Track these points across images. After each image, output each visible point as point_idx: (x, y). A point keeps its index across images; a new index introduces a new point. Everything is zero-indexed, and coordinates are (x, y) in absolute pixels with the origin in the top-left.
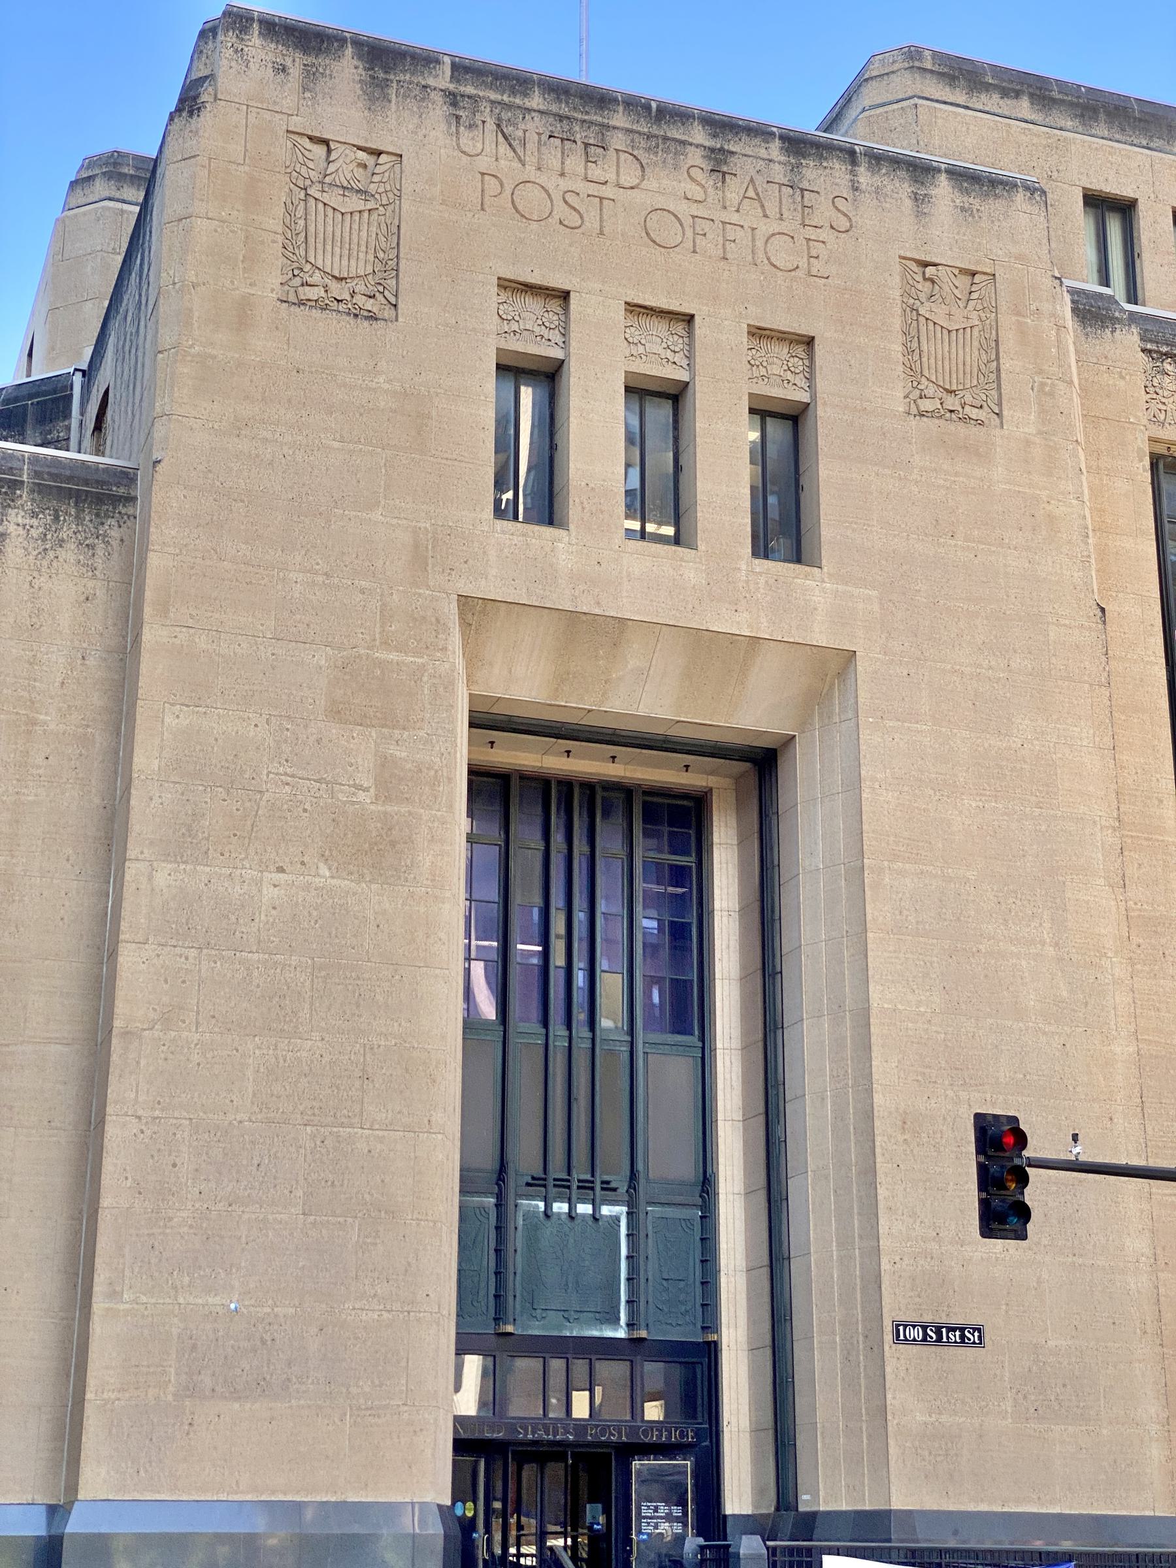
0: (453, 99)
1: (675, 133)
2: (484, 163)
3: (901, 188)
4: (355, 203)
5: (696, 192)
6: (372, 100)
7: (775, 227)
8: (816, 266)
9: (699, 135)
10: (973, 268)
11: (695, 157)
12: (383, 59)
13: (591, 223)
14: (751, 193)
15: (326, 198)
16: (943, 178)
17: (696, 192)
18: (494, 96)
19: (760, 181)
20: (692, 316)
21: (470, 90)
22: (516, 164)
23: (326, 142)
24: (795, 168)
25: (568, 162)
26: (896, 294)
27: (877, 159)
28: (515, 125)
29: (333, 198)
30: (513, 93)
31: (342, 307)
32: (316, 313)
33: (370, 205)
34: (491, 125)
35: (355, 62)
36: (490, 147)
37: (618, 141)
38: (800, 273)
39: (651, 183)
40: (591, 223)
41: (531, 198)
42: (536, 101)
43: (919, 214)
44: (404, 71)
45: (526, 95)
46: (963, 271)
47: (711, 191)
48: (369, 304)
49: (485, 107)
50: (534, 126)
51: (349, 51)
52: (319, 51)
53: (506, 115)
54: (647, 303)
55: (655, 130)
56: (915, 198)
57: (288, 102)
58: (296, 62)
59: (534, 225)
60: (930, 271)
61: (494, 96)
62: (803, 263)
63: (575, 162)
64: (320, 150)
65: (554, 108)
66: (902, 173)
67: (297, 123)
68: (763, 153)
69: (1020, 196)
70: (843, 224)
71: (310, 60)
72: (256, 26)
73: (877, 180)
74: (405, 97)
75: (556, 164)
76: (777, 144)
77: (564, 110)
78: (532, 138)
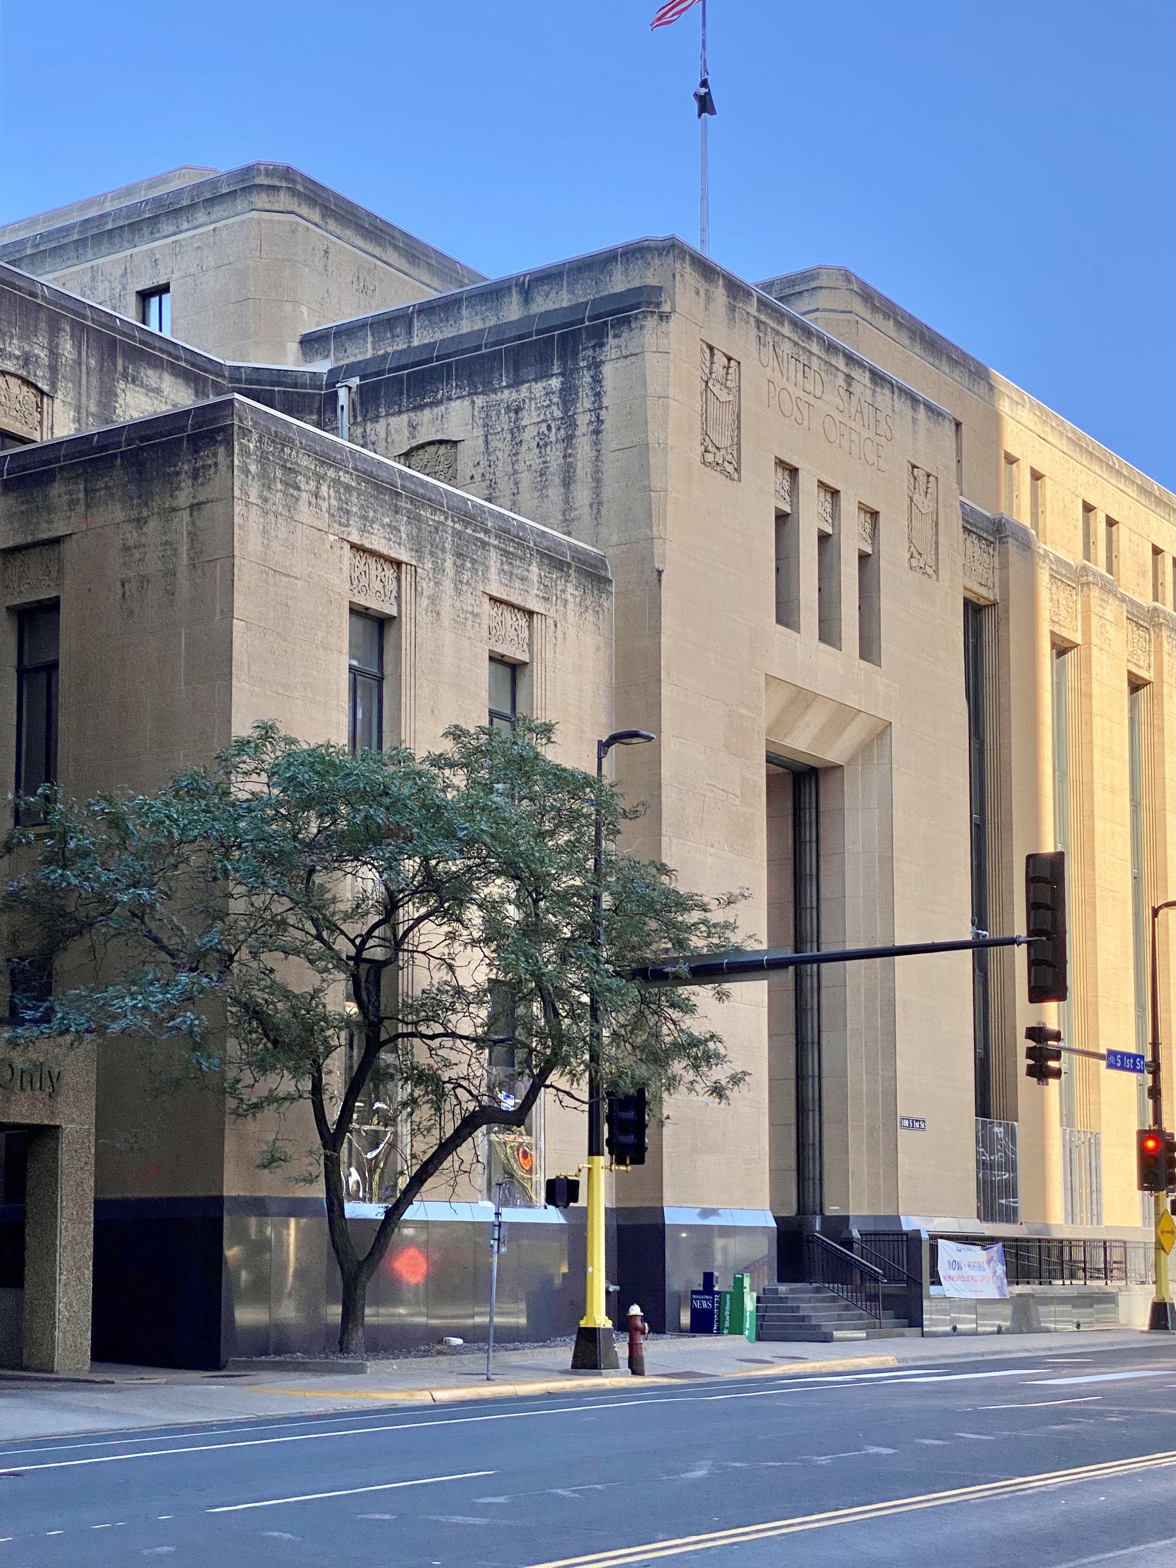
20: (838, 491)
21: (763, 318)
23: (711, 348)
31: (719, 469)
38: (875, 467)
40: (806, 423)
45: (782, 324)
50: (786, 348)
53: (777, 339)
66: (909, 402)
76: (867, 374)
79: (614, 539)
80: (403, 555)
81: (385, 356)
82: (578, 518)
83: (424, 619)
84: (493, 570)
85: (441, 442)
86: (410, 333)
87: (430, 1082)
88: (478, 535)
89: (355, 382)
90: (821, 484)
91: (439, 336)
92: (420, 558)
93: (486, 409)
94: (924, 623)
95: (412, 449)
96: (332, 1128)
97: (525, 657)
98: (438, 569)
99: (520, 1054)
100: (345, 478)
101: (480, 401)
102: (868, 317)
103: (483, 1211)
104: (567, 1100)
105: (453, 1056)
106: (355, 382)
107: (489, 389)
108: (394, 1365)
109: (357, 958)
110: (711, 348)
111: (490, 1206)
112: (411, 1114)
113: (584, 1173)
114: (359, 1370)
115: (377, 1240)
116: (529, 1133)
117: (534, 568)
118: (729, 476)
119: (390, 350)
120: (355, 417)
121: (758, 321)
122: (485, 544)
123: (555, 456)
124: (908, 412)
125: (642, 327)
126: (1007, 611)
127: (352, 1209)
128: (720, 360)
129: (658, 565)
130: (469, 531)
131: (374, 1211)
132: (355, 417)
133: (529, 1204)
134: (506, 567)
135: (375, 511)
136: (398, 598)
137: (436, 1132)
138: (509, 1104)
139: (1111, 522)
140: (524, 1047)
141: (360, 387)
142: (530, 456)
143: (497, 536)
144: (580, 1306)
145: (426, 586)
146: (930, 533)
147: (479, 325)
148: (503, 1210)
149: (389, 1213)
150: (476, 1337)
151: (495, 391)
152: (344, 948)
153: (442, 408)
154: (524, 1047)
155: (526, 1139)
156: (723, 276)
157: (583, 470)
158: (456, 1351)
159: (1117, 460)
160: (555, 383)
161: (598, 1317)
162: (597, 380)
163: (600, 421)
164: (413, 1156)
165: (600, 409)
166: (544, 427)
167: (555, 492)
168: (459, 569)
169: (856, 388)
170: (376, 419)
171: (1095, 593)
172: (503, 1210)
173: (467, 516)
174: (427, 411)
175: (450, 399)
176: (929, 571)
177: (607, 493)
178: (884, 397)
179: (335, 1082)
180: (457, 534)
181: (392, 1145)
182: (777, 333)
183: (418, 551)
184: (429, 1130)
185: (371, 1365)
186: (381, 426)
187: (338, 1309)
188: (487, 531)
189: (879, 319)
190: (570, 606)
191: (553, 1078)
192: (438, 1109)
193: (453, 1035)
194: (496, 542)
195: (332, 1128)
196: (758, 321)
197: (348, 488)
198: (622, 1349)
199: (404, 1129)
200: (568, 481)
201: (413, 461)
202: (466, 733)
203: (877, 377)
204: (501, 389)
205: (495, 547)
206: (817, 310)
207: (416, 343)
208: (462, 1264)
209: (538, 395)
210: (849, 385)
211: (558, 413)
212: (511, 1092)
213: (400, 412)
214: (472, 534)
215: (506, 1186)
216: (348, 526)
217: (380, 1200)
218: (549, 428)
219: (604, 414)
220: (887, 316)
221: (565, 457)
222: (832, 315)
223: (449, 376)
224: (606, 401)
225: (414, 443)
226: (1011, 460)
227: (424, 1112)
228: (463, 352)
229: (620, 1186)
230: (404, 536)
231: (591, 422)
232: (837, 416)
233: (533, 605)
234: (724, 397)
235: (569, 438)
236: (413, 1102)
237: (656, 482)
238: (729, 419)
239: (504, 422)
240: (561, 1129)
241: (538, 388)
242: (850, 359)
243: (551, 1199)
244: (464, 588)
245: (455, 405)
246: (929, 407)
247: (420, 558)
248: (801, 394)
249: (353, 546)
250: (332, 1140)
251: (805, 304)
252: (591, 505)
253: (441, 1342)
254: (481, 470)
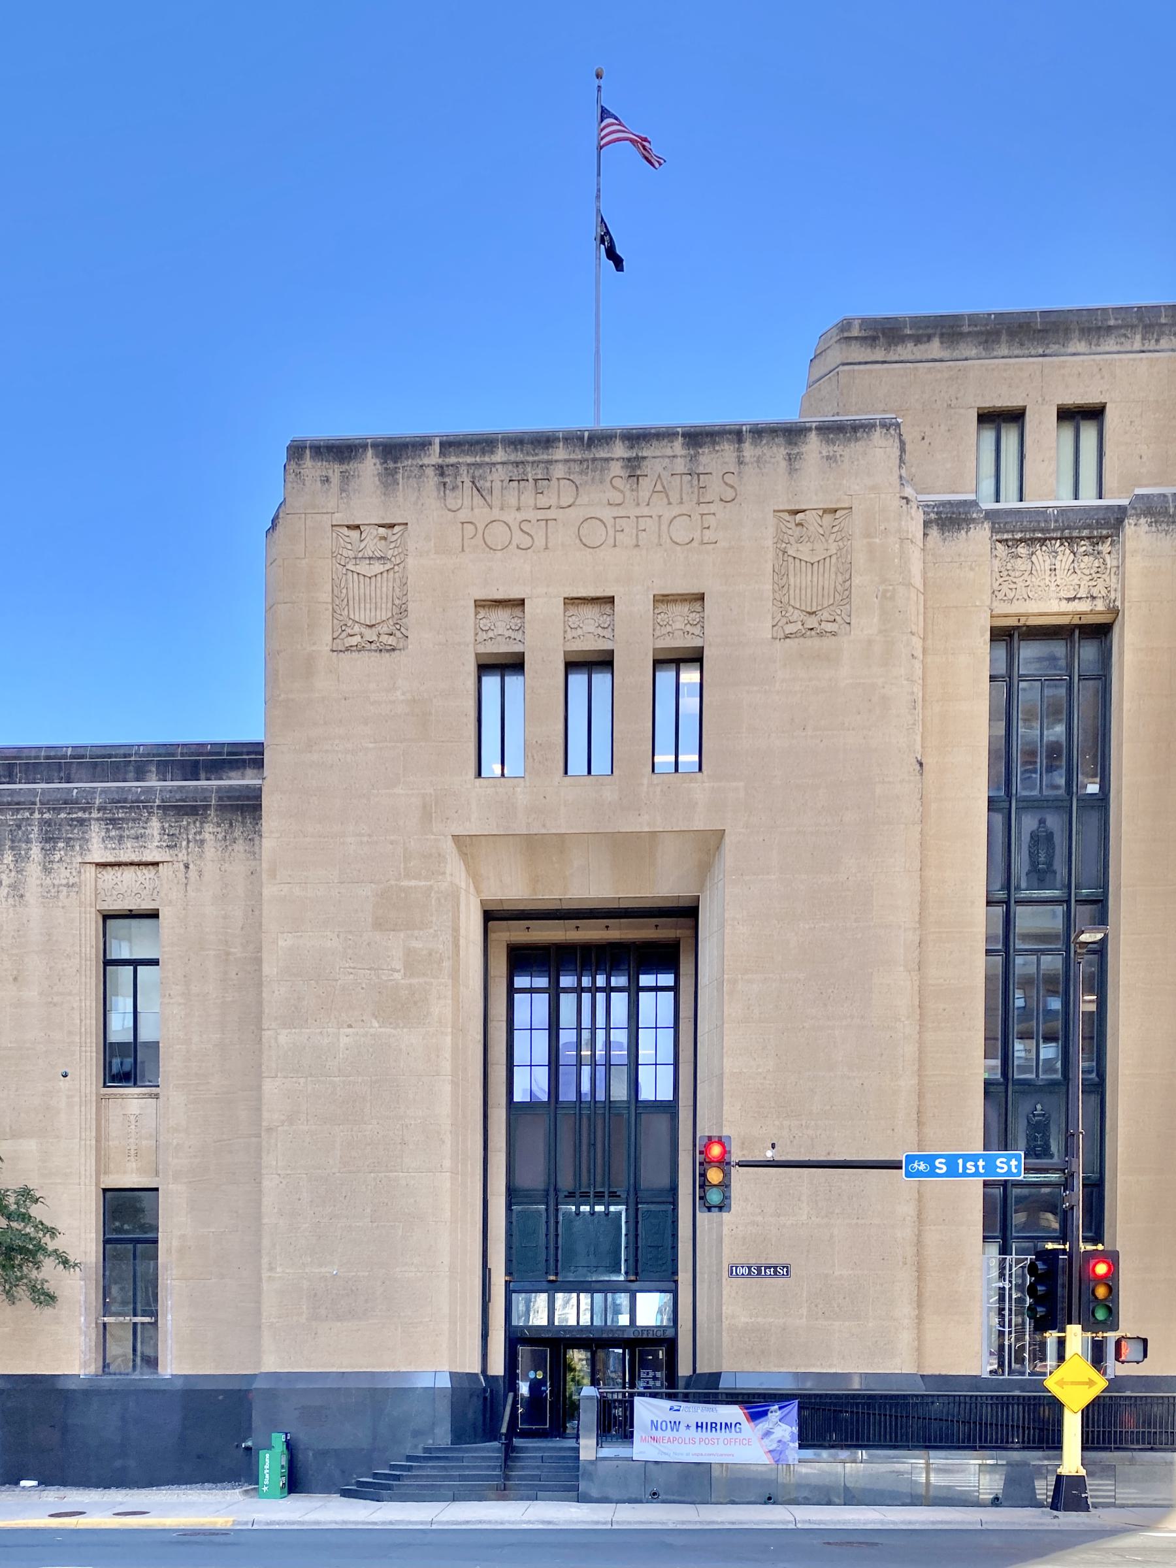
0: (441, 470)
1: (602, 453)
2: (463, 515)
3: (777, 452)
4: (378, 567)
5: (617, 497)
6: (386, 485)
7: (676, 510)
8: (709, 535)
9: (620, 450)
10: (834, 506)
11: (616, 469)
12: (393, 451)
13: (540, 542)
14: (659, 488)
15: (358, 569)
16: (813, 437)
17: (617, 497)
18: (469, 460)
19: (665, 475)
21: (453, 460)
22: (487, 509)
24: (693, 458)
25: (522, 498)
26: (769, 543)
27: (759, 432)
28: (485, 479)
29: (363, 568)
30: (483, 453)
32: (355, 655)
33: (388, 566)
34: (468, 484)
35: (374, 461)
36: (467, 502)
37: (559, 471)
39: (584, 499)
40: (540, 542)
41: (498, 534)
42: (500, 455)
43: (792, 471)
44: (407, 458)
46: (825, 511)
47: (628, 493)
48: (391, 640)
49: (463, 470)
51: (370, 452)
52: (350, 459)
54: (580, 595)
55: (588, 455)
56: (790, 458)
57: (332, 504)
58: (334, 470)
59: (499, 554)
60: (800, 516)
61: (469, 460)
62: (697, 535)
63: (528, 498)
64: (355, 534)
65: (513, 458)
66: (780, 440)
67: (339, 518)
68: (669, 452)
69: (877, 434)
70: (730, 493)
71: (345, 467)
72: (308, 451)
73: (758, 451)
74: (409, 477)
75: (513, 501)
77: (520, 457)
78: (497, 485)
88: (74, 816)
122: (82, 822)
130: (63, 815)
134: (113, 833)
156: (375, 446)
194: (100, 815)
248: (532, 515)
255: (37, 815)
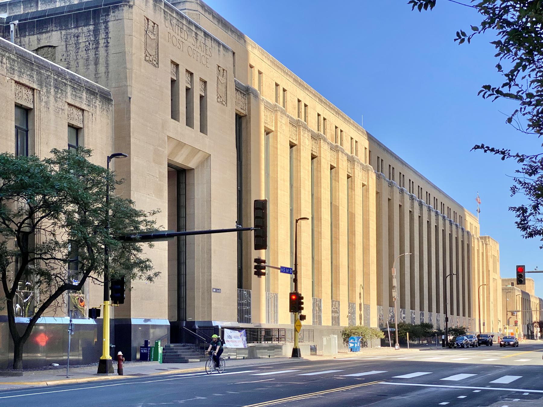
11: (194, 33)
21: (166, 10)
23: (148, 19)
50: (174, 21)
79: (114, 85)
80: (35, 86)
81: (28, 13)
82: (101, 77)
83: (43, 110)
84: (69, 94)
85: (50, 46)
86: (37, 5)
87: (47, 275)
89: (17, 22)
90: (187, 71)
91: (48, 7)
92: (41, 88)
93: (66, 35)
94: (221, 121)
95: (39, 48)
96: (10, 291)
97: (81, 126)
98: (48, 92)
99: (80, 265)
100: (12, 57)
101: (64, 32)
102: (203, 13)
103: (66, 320)
104: (96, 282)
105: (55, 266)
106: (17, 22)
107: (67, 28)
108: (34, 373)
109: (19, 231)
110: (148, 19)
111: (69, 318)
112: (39, 286)
113: (102, 307)
114: (20, 375)
115: (27, 330)
116: (83, 293)
117: (84, 94)
118: (154, 65)
119: (30, 11)
120: (17, 35)
121: (164, 11)
122: (66, 84)
123: (92, 54)
124: (217, 48)
125: (123, 10)
126: (250, 118)
127: (18, 320)
128: (151, 24)
129: (129, 96)
130: (60, 79)
131: (26, 320)
132: (17, 35)
133: (83, 318)
134: (74, 93)
135: (24, 69)
136: (33, 102)
137: (49, 293)
138: (76, 283)
139: (284, 90)
140: (81, 262)
141: (19, 24)
142: (82, 53)
143: (70, 82)
144: (100, 352)
145: (44, 98)
146: (224, 90)
147: (63, 5)
148: (73, 320)
149: (31, 320)
150: (63, 363)
151: (69, 29)
152: (14, 227)
153: (50, 34)
154: (81, 262)
155: (82, 295)
157: (102, 60)
158: (56, 368)
159: (286, 69)
160: (91, 27)
161: (107, 355)
162: (107, 28)
163: (108, 43)
164: (40, 301)
165: (108, 38)
166: (87, 43)
167: (92, 67)
168: (56, 93)
169: (199, 38)
170: (25, 36)
171: (279, 114)
172: (73, 320)
173: (59, 73)
174: (44, 35)
175: (52, 31)
176: (224, 103)
177: (111, 69)
178: (209, 42)
179: (11, 274)
180: (56, 80)
181: (33, 298)
182: (171, 16)
183: (41, 85)
184: (46, 292)
185: (25, 373)
186: (27, 39)
187: (13, 354)
188: (66, 80)
189: (207, 14)
190: (98, 108)
191: (92, 274)
192: (49, 285)
193: (55, 258)
195: (10, 291)
196: (164, 11)
197: (14, 60)
198: (115, 366)
199: (37, 291)
200: (96, 64)
201: (39, 53)
202: (59, 152)
203: (206, 34)
204: (72, 28)
205: (70, 85)
206: (185, 9)
207: (39, 9)
208: (59, 337)
209: (85, 32)
210: (197, 36)
211: (92, 39)
212: (77, 279)
213: (34, 35)
214: (61, 81)
215: (74, 311)
216: (14, 74)
217: (28, 316)
218: (89, 44)
219: (109, 40)
220: (209, 13)
221: (95, 54)
222: (191, 12)
223: (52, 23)
224: (110, 35)
225: (39, 46)
226: (251, 67)
227: (44, 286)
228: (57, 14)
229: (116, 310)
230: (35, 79)
231: (104, 43)
232: (193, 47)
233: (84, 107)
234: (152, 37)
235: (97, 48)
236: (40, 282)
237: (128, 66)
238: (154, 45)
239: (73, 41)
240: (94, 291)
241: (85, 29)
242: (197, 27)
243: (90, 316)
244: (58, 99)
245: (54, 33)
246: (224, 46)
247: (41, 88)
248: (180, 38)
249: (16, 82)
250: (10, 295)
251: (181, 6)
252: (105, 72)
253: (51, 365)
254: (64, 57)
255: (52, 75)
